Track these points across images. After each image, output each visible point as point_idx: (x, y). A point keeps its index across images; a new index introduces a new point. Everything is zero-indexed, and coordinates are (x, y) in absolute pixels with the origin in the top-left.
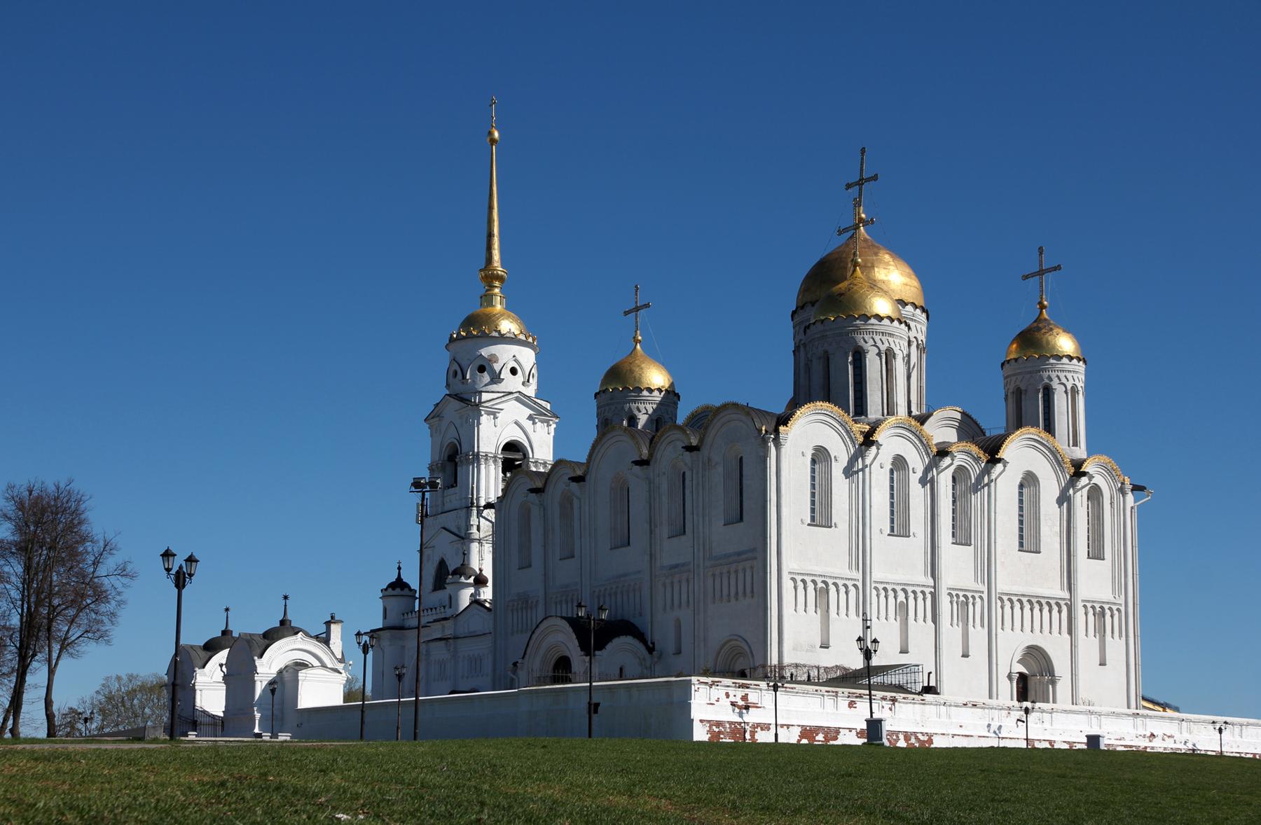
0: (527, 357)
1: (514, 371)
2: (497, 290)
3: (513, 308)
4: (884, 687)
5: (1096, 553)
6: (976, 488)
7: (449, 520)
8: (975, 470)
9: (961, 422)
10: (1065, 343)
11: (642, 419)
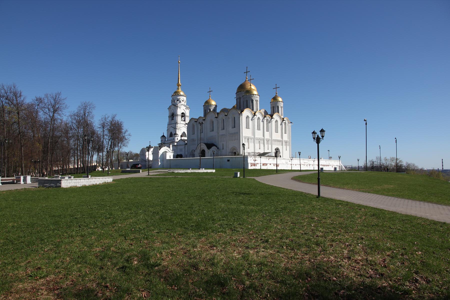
0: (185, 98)
3: (182, 90)
4: (268, 156)
5: (285, 133)
6: (269, 123)
7: (173, 125)
8: (269, 119)
10: (280, 99)
11: (212, 110)
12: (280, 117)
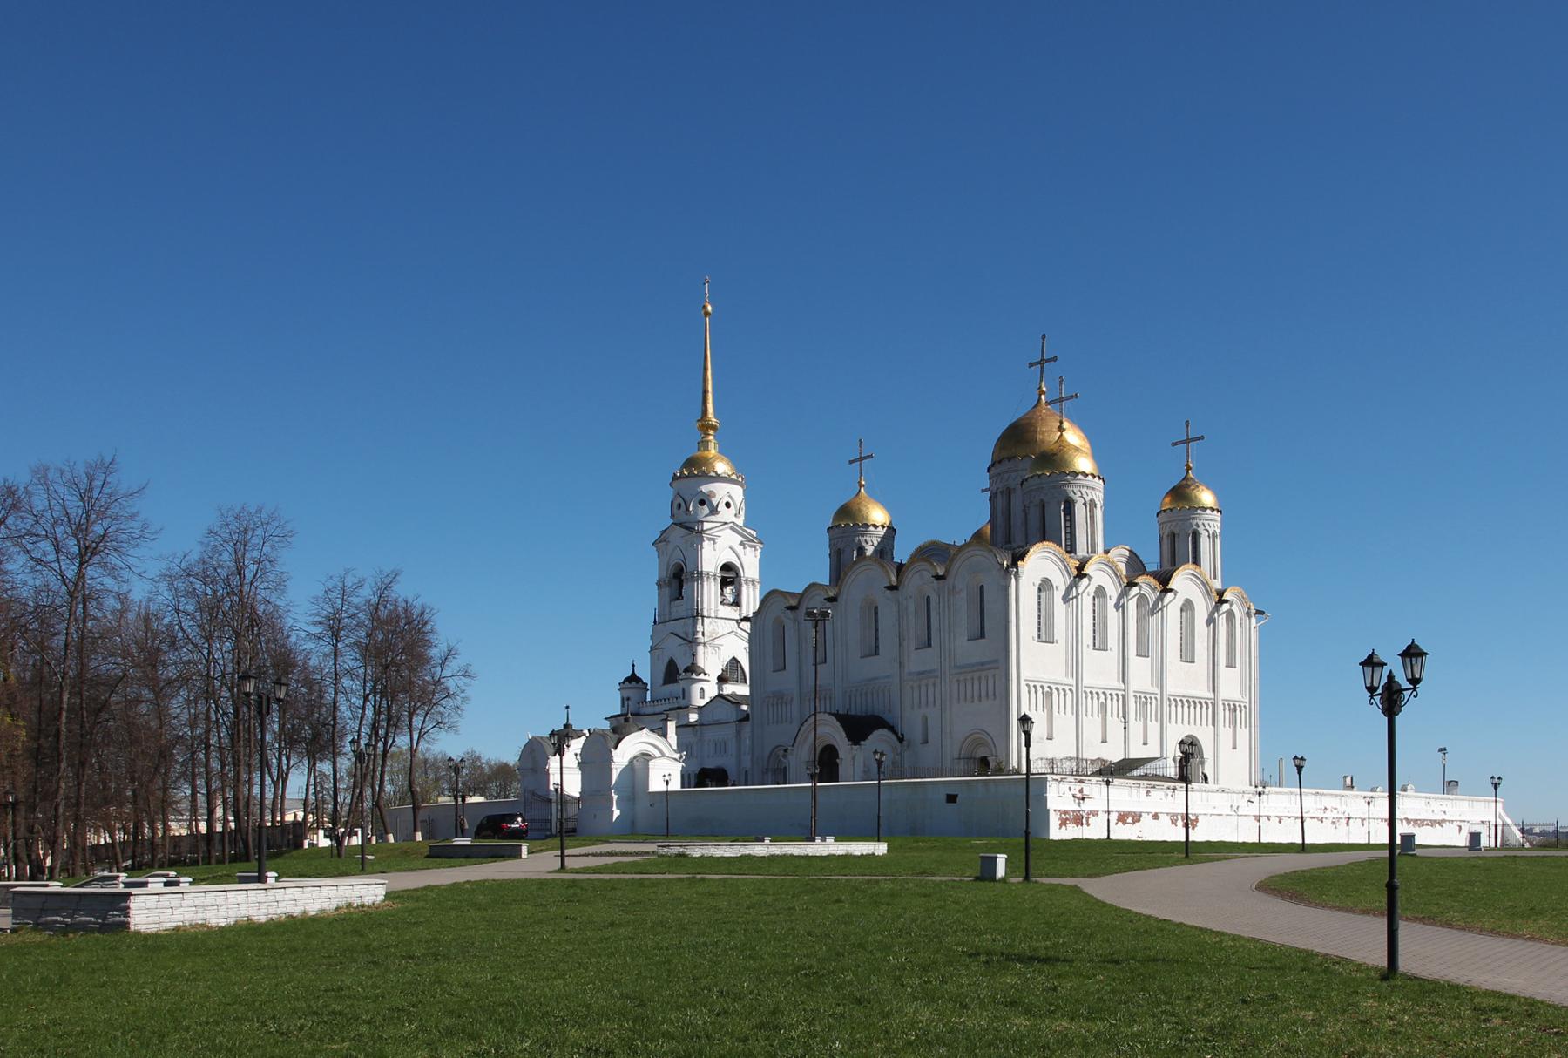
0: (737, 493)
1: (728, 505)
4: (1145, 777)
5: (1231, 664)
6: (1153, 612)
7: (677, 627)
8: (1152, 597)
9: (1129, 558)
11: (870, 550)
12: (1205, 585)
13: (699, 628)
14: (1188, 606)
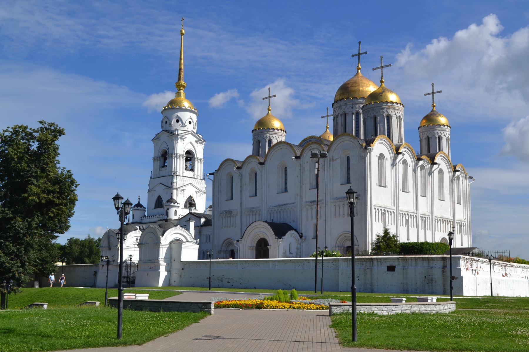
0: (194, 117)
1: (190, 123)
2: (182, 91)
3: (187, 98)
7: (163, 180)
10: (442, 120)
13: (175, 180)
14: (441, 172)
